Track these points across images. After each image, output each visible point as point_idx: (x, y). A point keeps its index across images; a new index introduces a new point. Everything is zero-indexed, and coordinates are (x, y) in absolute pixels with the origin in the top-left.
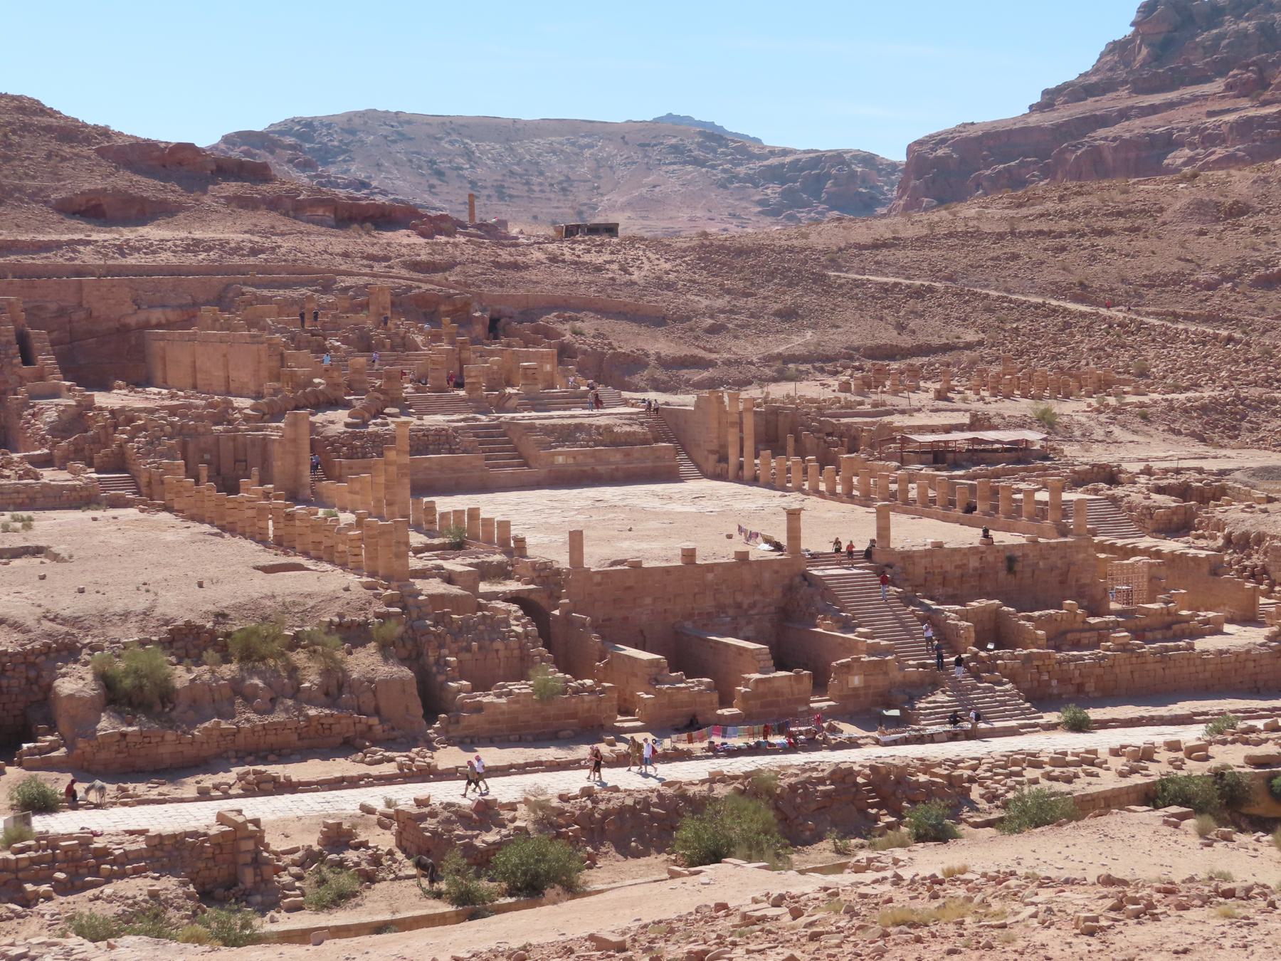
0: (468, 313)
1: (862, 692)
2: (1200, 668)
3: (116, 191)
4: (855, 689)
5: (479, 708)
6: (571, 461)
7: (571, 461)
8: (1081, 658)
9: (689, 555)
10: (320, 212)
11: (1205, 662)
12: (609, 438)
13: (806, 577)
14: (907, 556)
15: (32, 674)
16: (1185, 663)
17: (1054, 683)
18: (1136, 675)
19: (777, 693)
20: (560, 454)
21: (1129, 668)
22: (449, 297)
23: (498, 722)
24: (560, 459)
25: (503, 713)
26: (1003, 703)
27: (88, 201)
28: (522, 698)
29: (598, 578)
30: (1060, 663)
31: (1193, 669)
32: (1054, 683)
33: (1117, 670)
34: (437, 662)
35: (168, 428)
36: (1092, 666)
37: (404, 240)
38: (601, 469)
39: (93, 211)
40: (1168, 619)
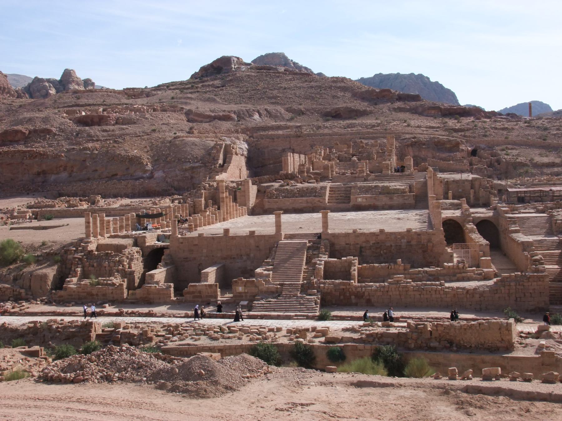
1: (244, 295)
2: (443, 296)
3: (347, 108)
4: (240, 293)
7: (364, 200)
8: (372, 286)
10: (433, 112)
11: (446, 293)
12: (387, 192)
14: (334, 235)
16: (433, 293)
17: (353, 297)
19: (200, 292)
20: (360, 197)
21: (398, 293)
23: (72, 295)
24: (360, 200)
25: (74, 292)
26: (303, 304)
28: (82, 286)
31: (438, 296)
33: (390, 293)
36: (376, 291)
38: (379, 203)
39: (336, 115)
40: (457, 271)
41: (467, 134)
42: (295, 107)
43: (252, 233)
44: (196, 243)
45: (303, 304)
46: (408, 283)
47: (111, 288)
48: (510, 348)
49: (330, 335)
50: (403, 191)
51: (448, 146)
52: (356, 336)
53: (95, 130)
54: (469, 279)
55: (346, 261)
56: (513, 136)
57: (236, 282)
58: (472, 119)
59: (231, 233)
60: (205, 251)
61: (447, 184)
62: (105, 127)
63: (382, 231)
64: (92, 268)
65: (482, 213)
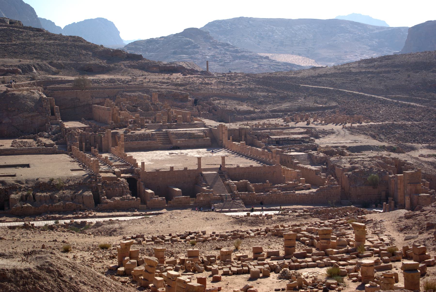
0: (187, 98)
5: (107, 203)
6: (182, 142)
7: (182, 142)
11: (297, 196)
13: (202, 175)
15: (6, 193)
18: (278, 199)
22: (182, 94)
26: (237, 205)
27: (88, 67)
29: (148, 174)
30: (257, 195)
32: (255, 200)
34: (101, 192)
35: (77, 134)
37: (177, 77)
44: (157, 174)
45: (237, 205)
46: (280, 192)
47: (133, 201)
51: (180, 97)
55: (243, 182)
57: (199, 195)
59: (175, 169)
60: (161, 179)
64: (110, 191)
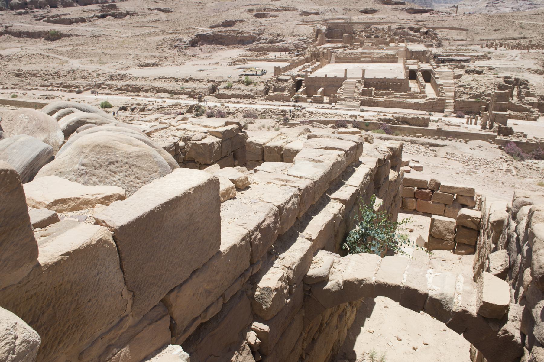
9: (326, 75)
14: (367, 79)
39: (366, 12)
41: (425, 23)
42: (348, 7)
43: (336, 76)
48: (427, 126)
49: (365, 118)
50: (393, 55)
52: (374, 119)
53: (263, 20)
54: (417, 98)
56: (446, 24)
58: (428, 14)
61: (412, 53)
62: (266, 19)
63: (385, 78)
65: (425, 66)
